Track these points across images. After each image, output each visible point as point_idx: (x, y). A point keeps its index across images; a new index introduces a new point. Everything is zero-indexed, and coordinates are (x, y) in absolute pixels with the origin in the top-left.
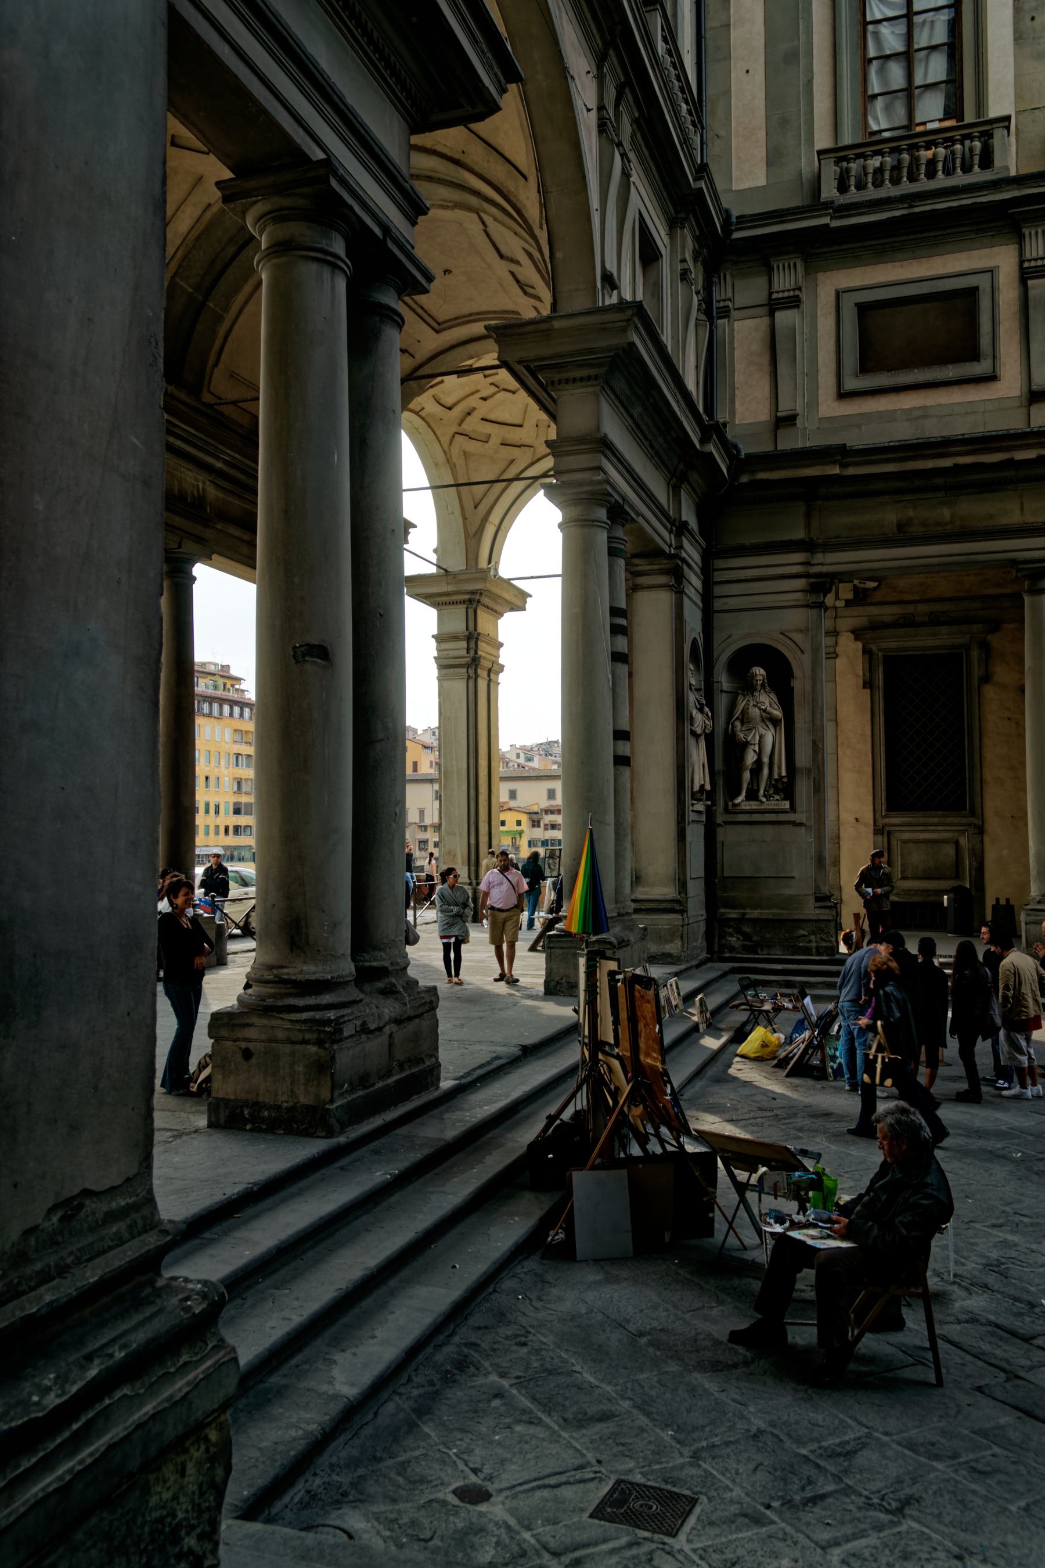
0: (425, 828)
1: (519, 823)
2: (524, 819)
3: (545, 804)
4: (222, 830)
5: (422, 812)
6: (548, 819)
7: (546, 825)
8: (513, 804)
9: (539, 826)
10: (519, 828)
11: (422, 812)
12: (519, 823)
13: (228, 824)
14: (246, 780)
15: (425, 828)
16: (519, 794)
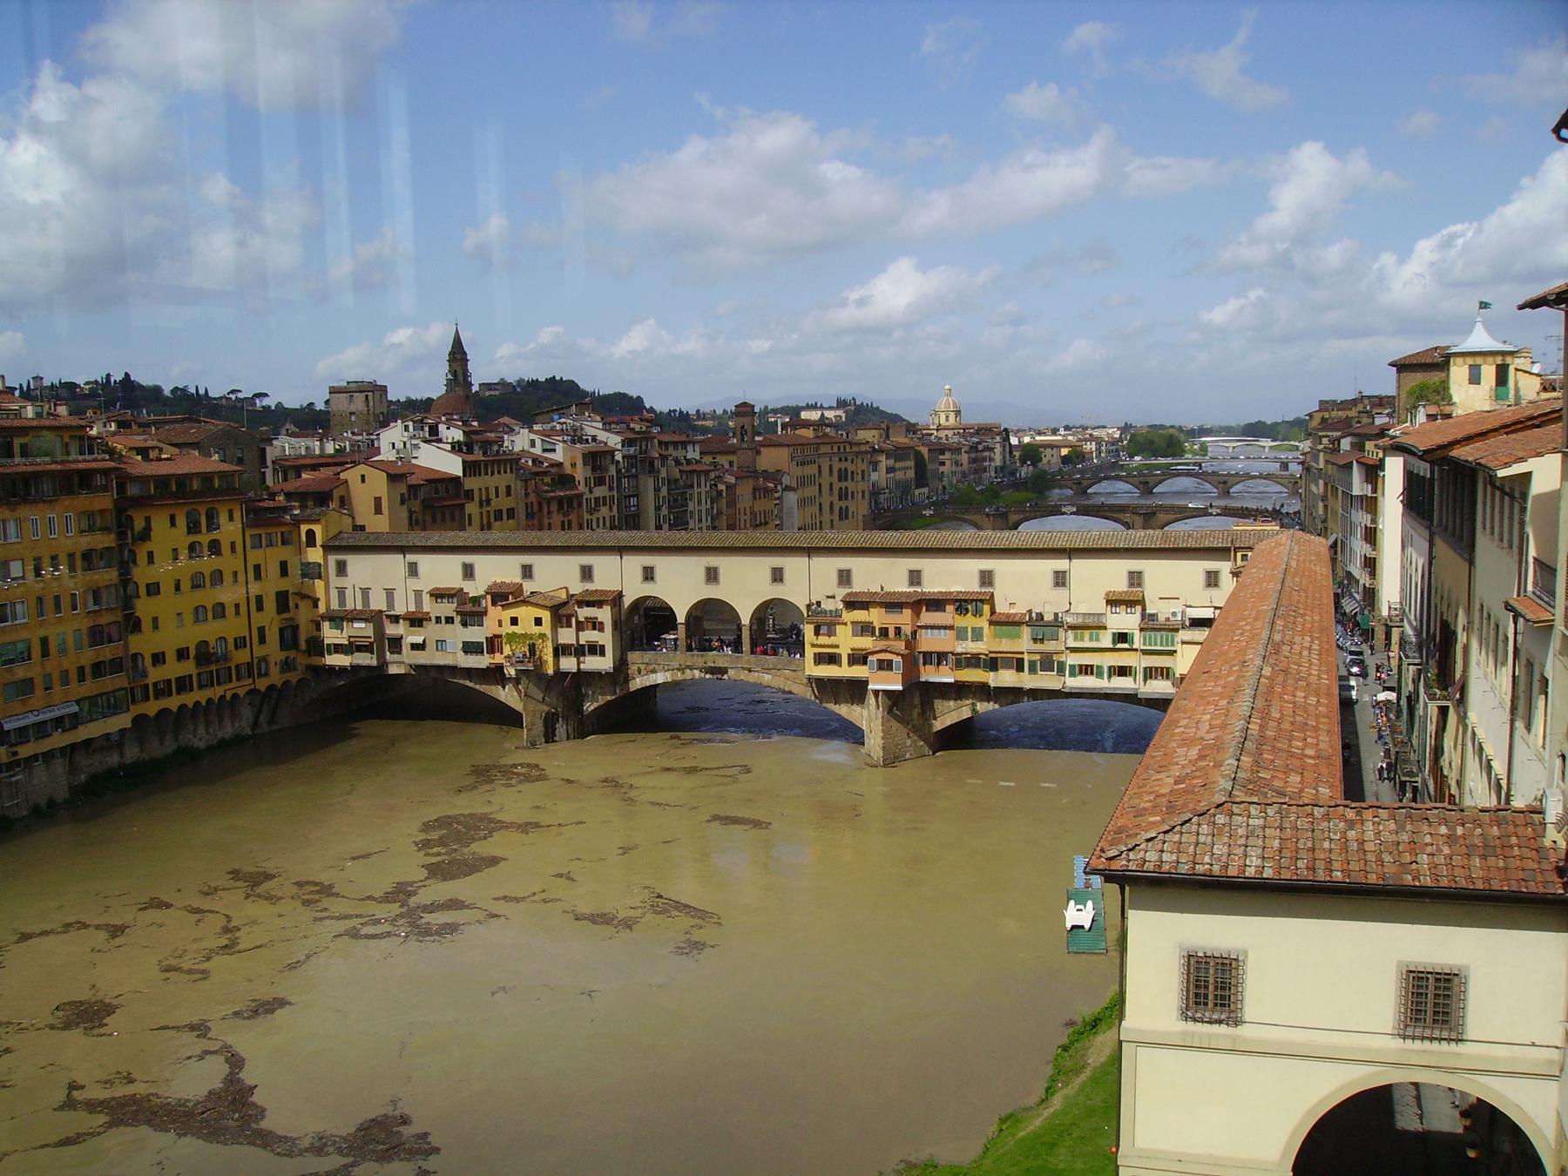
0: (395, 619)
1: (538, 622)
2: (546, 616)
3: (577, 588)
4: (73, 675)
5: (390, 593)
6: (584, 613)
7: (578, 623)
8: (528, 587)
9: (569, 626)
10: (537, 630)
11: (390, 593)
12: (538, 622)
13: (83, 662)
14: (107, 587)
15: (395, 619)
16: (535, 570)
